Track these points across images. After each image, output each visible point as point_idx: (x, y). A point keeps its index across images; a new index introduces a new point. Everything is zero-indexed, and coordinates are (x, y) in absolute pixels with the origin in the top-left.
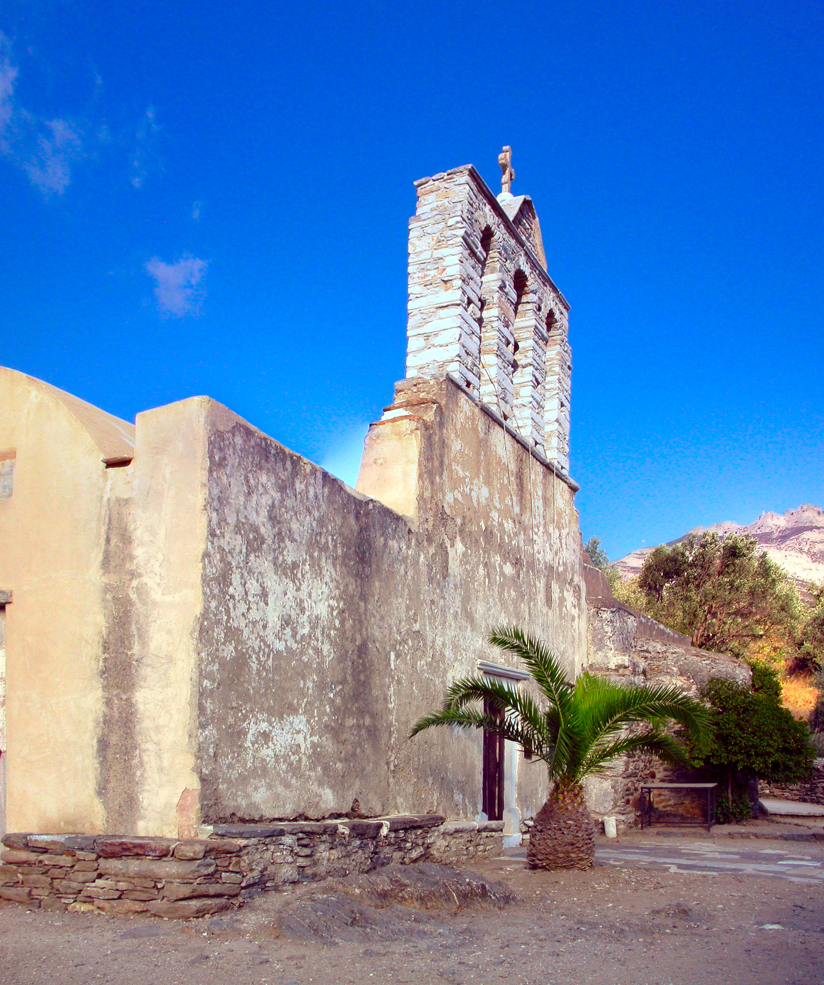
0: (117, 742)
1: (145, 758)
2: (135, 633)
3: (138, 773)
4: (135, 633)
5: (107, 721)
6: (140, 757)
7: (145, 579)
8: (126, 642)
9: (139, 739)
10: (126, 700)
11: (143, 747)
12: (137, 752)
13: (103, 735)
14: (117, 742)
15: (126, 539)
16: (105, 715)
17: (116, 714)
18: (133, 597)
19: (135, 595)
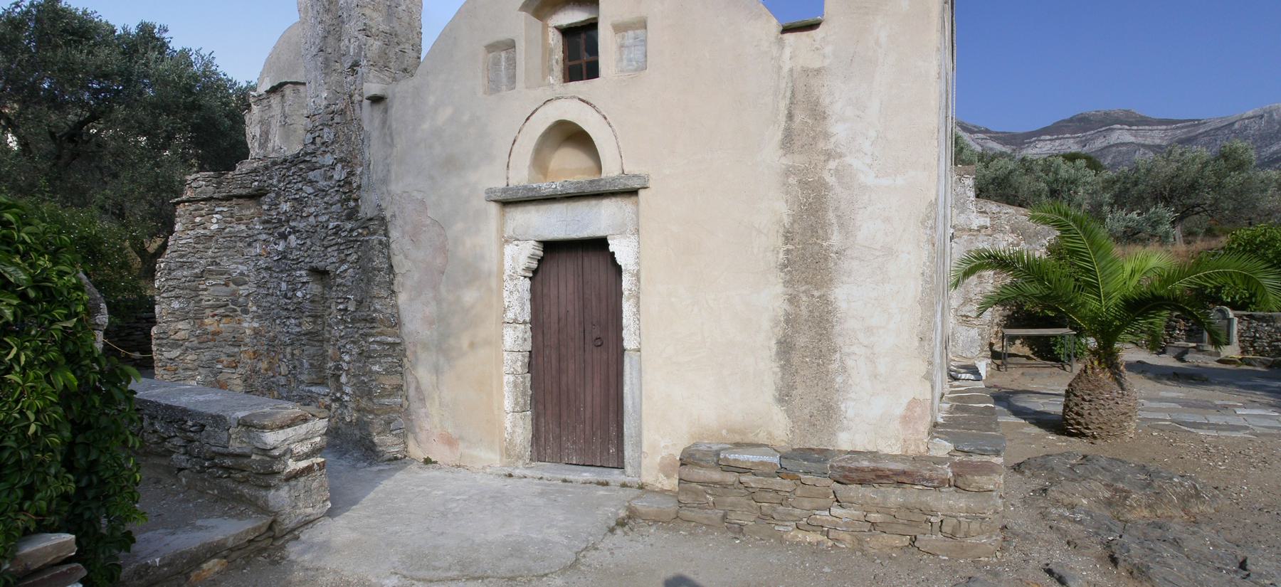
0: (807, 344)
1: (850, 363)
2: (834, 221)
3: (839, 379)
4: (834, 221)
5: (790, 320)
6: (842, 362)
7: (848, 160)
8: (820, 232)
9: (839, 341)
10: (819, 297)
11: (846, 349)
12: (838, 355)
13: (786, 335)
14: (807, 344)
15: (818, 113)
16: (787, 314)
17: (804, 312)
18: (831, 180)
19: (834, 179)
